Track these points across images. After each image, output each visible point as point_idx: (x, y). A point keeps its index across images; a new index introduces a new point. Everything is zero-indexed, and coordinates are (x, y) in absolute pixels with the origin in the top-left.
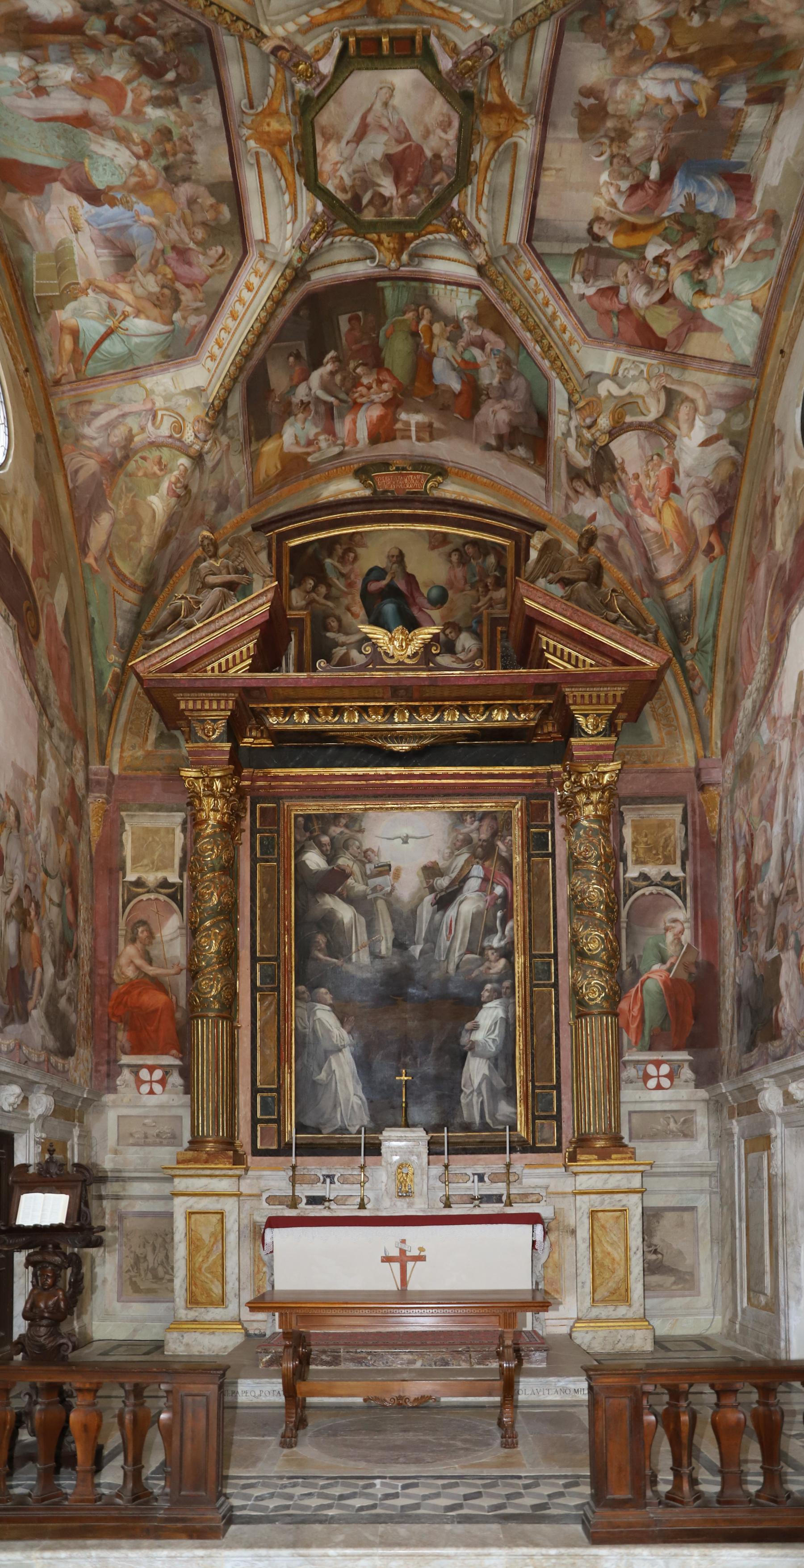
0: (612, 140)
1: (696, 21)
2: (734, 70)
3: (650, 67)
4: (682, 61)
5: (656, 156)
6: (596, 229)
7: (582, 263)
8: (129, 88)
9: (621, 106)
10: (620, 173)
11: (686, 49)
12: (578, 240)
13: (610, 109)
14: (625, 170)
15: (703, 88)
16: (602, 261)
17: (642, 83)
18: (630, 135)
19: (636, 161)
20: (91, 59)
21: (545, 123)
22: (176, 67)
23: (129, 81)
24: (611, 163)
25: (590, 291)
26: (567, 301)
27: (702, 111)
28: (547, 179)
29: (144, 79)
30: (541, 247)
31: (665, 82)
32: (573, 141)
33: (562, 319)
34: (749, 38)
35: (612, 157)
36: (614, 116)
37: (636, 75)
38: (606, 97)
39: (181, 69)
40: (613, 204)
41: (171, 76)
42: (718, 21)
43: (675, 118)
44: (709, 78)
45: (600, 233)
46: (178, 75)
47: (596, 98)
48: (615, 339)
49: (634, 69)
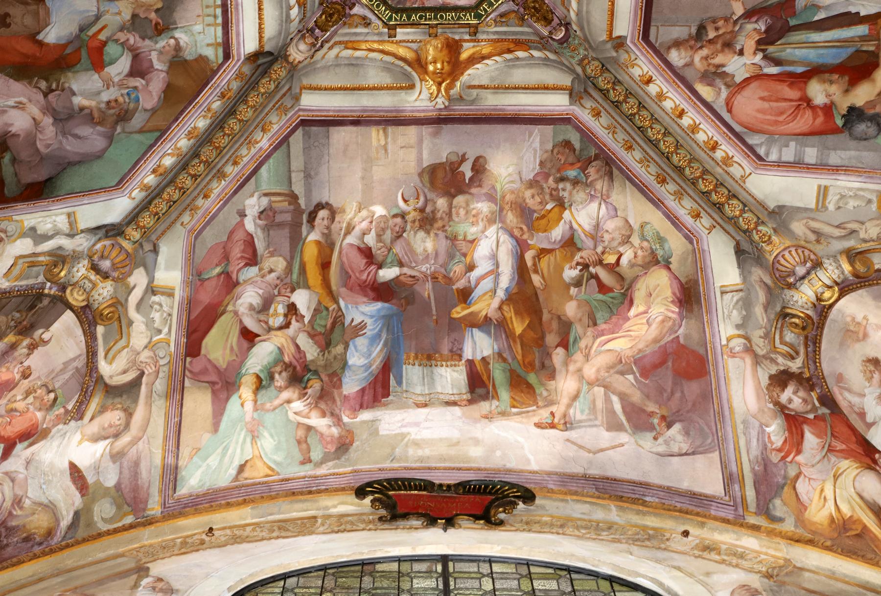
0: (422, 210)
2: (510, 335)
5: (405, 270)
6: (323, 214)
7: (282, 204)
9: (462, 212)
10: (383, 230)
12: (308, 191)
13: (460, 200)
14: (388, 236)
15: (485, 304)
16: (286, 232)
18: (428, 232)
19: (398, 249)
21: (440, 121)
24: (395, 216)
25: (250, 225)
26: (236, 192)
27: (459, 312)
28: (375, 134)
30: (297, 140)
31: (494, 257)
32: (420, 160)
33: (218, 188)
34: (551, 339)
35: (403, 215)
36: (450, 206)
38: (474, 190)
40: (349, 230)
43: (449, 281)
44: (500, 308)
45: (318, 221)
47: (471, 179)
48: (195, 276)
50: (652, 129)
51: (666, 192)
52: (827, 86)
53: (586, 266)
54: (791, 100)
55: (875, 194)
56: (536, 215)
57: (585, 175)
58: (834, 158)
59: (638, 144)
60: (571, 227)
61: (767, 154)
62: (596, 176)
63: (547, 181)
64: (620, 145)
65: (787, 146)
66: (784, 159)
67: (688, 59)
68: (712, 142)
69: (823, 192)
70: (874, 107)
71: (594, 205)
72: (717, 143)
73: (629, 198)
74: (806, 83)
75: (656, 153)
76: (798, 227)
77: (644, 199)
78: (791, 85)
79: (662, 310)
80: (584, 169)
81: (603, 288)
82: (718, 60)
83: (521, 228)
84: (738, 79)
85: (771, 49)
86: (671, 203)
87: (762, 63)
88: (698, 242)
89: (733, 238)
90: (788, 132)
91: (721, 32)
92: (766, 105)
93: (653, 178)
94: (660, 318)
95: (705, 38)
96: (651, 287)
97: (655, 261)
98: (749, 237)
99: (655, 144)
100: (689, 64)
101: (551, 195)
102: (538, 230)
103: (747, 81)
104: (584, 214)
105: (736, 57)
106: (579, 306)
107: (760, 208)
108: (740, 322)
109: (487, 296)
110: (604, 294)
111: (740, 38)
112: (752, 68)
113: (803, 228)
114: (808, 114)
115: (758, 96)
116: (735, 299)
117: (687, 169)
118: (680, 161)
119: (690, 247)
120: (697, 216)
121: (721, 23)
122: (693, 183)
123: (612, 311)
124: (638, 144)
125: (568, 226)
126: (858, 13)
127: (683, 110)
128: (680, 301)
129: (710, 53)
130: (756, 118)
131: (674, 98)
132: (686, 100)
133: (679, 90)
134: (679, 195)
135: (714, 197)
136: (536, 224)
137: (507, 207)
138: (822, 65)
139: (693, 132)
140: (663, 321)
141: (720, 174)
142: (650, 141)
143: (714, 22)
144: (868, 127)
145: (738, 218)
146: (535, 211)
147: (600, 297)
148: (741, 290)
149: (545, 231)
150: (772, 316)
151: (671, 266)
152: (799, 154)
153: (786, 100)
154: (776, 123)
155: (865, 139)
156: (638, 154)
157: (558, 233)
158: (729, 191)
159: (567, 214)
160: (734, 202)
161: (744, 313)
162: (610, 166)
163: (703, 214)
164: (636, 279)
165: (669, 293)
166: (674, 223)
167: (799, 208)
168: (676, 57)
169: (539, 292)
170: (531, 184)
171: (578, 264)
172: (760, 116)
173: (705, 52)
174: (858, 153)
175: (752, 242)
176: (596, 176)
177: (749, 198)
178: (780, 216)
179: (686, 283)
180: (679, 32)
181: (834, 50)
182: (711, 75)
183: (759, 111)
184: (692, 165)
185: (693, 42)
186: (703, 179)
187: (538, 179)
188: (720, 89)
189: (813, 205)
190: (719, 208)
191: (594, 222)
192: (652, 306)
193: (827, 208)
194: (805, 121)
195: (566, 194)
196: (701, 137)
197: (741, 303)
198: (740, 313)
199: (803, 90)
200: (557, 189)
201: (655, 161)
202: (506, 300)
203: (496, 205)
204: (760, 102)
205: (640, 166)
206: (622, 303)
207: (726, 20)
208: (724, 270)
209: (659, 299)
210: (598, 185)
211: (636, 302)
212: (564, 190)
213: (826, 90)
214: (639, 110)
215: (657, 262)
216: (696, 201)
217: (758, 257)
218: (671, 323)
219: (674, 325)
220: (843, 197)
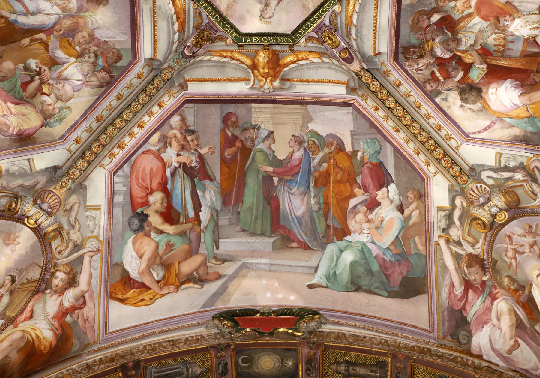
1: (33, 63)
3: (55, 24)
4: (31, 31)
8: (472, 10)
11: (32, 41)
17: (57, 10)
20: (492, 40)
22: (429, 26)
23: (470, 15)
29: (456, 16)
37: (64, 17)
39: (426, 23)
41: (436, 18)
42: (16, 65)
46: (429, 19)
49: (67, 23)
50: (130, 113)
51: (91, 122)
52: (160, 201)
53: (39, 73)
54: (151, 185)
55: (97, 234)
56: (71, 39)
57: (100, 70)
58: (118, 211)
59: (120, 104)
60: (64, 63)
61: (118, 176)
62: (99, 77)
63: (94, 46)
64: (120, 92)
65: (123, 186)
66: (116, 185)
67: (174, 126)
68: (124, 145)
69: (97, 208)
70: (148, 226)
71: (80, 77)
72: (124, 148)
73: (87, 98)
74: (161, 191)
75: (115, 116)
76: (74, 199)
77: (86, 108)
78: (160, 183)
79: (14, 123)
80: (104, 69)
81: (25, 86)
82: (174, 143)
83: (61, 30)
84: (163, 155)
85: (181, 170)
86: (85, 125)
87: (172, 167)
88: (60, 142)
89: (64, 165)
90: (132, 185)
91: (191, 143)
92: (148, 172)
93: (100, 113)
94: (8, 123)
95: (187, 134)
96: (29, 116)
97: (47, 118)
98: (65, 175)
99: (120, 115)
100: (171, 127)
101: (86, 49)
102: (60, 41)
103: (162, 160)
104: (74, 71)
105: (176, 153)
106: (10, 70)
107: (84, 178)
108: (10, 171)
109: (10, 8)
110: (21, 86)
111: (187, 153)
112: (169, 162)
113: (74, 202)
114: (144, 194)
115: (153, 166)
116: (25, 167)
117: (105, 136)
118: (110, 131)
119: (57, 138)
120: (77, 142)
121: (196, 142)
122: (96, 140)
123: (10, 92)
124: (120, 104)
125: (65, 61)
126: (201, 211)
127: (143, 127)
128: (21, 134)
129: (178, 138)
130: (140, 167)
131: (150, 122)
132: (149, 128)
133: (156, 123)
134: (89, 130)
135: (88, 153)
136: (65, 40)
137: (75, 20)
138: (172, 198)
139: (129, 135)
140: (6, 124)
141: (103, 153)
142: (122, 112)
143: (196, 139)
144: (136, 225)
145: (76, 168)
146: (73, 39)
147: (19, 84)
148: (31, 170)
149: (61, 46)
150: (16, 190)
151: (44, 127)
152: (119, 193)
153: (151, 182)
154: (137, 178)
155: (129, 225)
156: (114, 103)
157: (60, 54)
158: (93, 161)
159: (73, 60)
160: (86, 165)
161: (17, 173)
162: (107, 85)
163: (79, 145)
164: (34, 106)
165: (26, 127)
166: (72, 127)
167: (86, 197)
168: (176, 120)
169: (17, 43)
170: (92, 35)
171: (40, 68)
172: (141, 169)
173: (179, 135)
174: (121, 222)
175: (62, 177)
176: (99, 77)
177: (90, 171)
178: (81, 188)
179: (33, 137)
180: (190, 120)
181: (180, 202)
182: (165, 140)
183: (144, 168)
184: (108, 138)
185: (184, 128)
186: (99, 146)
187: (96, 40)
188: (157, 146)
189: (88, 204)
190: (82, 156)
191: (69, 77)
192: (16, 117)
193: (87, 211)
194: (139, 193)
195: (86, 59)
196: (127, 139)
197: (23, 171)
198: (17, 171)
199: (157, 190)
200: (89, 52)
201: (110, 114)
202: (9, 21)
203: (75, 13)
204: (150, 168)
205: (107, 104)
206: (16, 98)
207: (198, 145)
208: (43, 160)
209: (21, 121)
210: (94, 79)
211: (18, 106)
212: (89, 57)
213: (157, 201)
214: (141, 104)
215: (46, 119)
216: (86, 141)
217: (52, 181)
218: (5, 129)
219: (5, 131)
220: (95, 218)
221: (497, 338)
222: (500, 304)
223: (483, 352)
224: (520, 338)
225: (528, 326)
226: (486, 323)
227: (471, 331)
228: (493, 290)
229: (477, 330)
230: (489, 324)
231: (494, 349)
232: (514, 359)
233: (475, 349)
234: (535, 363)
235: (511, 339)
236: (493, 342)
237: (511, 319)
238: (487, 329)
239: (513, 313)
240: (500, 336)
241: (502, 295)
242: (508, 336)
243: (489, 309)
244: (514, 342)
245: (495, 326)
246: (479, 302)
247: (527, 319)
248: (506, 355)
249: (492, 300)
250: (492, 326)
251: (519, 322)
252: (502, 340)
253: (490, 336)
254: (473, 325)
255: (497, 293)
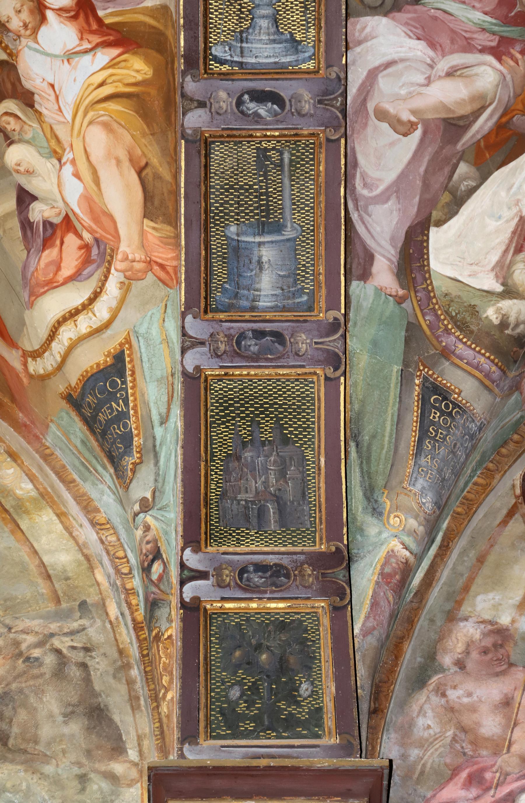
221: (404, 79)
222: (489, 70)
223: (358, 49)
224: (425, 133)
225: (459, 146)
226: (432, 45)
227: (399, 11)
228: (518, 47)
229: (406, 24)
230: (431, 53)
231: (373, 75)
232: (369, 130)
233: (358, 27)
234: (380, 180)
235: (414, 112)
236: (390, 70)
237: (461, 103)
238: (419, 49)
239: (476, 106)
240: (412, 84)
241: (511, 70)
242: (418, 103)
243: (468, 47)
244: (409, 121)
245: (432, 67)
246: (478, 16)
247: (475, 140)
248: (371, 106)
249: (492, 48)
250: (429, 61)
251: (461, 123)
252: (403, 92)
253: (402, 60)
254: (415, 12)
255: (512, 57)
